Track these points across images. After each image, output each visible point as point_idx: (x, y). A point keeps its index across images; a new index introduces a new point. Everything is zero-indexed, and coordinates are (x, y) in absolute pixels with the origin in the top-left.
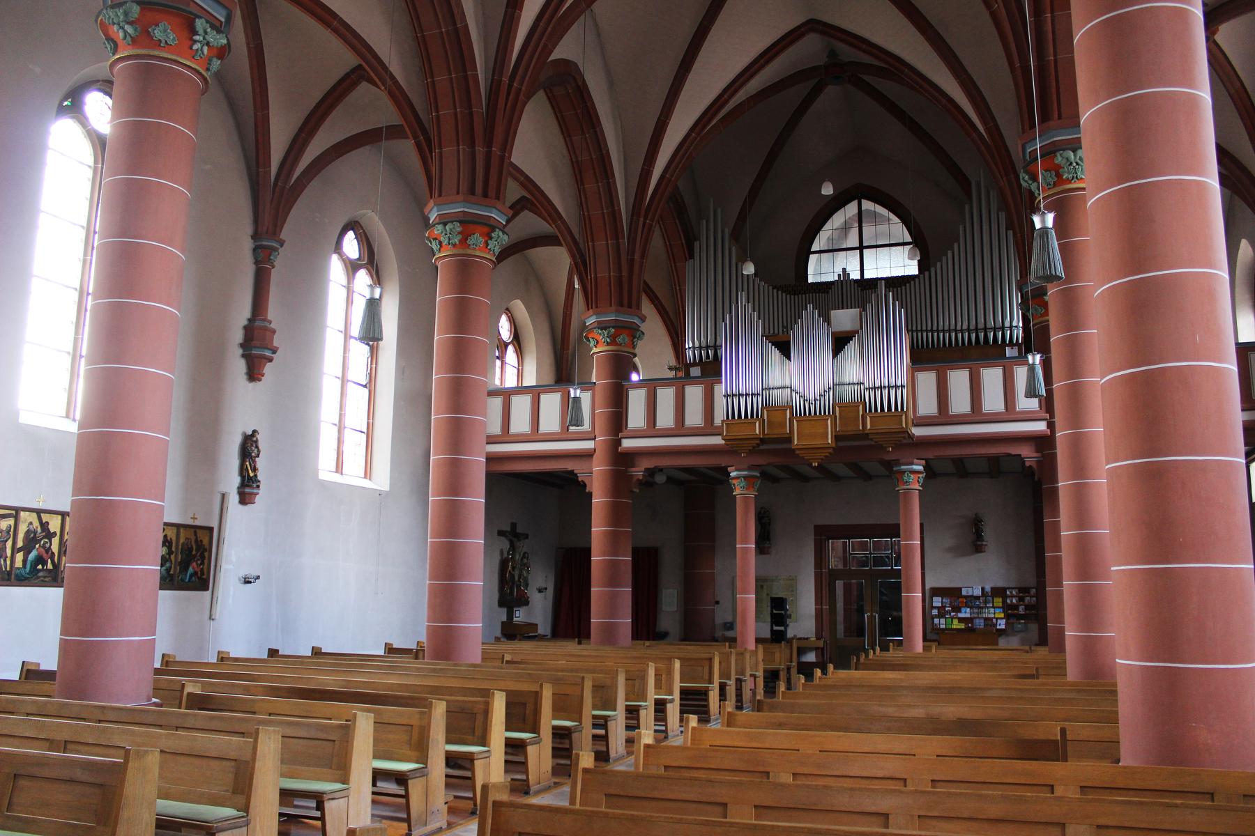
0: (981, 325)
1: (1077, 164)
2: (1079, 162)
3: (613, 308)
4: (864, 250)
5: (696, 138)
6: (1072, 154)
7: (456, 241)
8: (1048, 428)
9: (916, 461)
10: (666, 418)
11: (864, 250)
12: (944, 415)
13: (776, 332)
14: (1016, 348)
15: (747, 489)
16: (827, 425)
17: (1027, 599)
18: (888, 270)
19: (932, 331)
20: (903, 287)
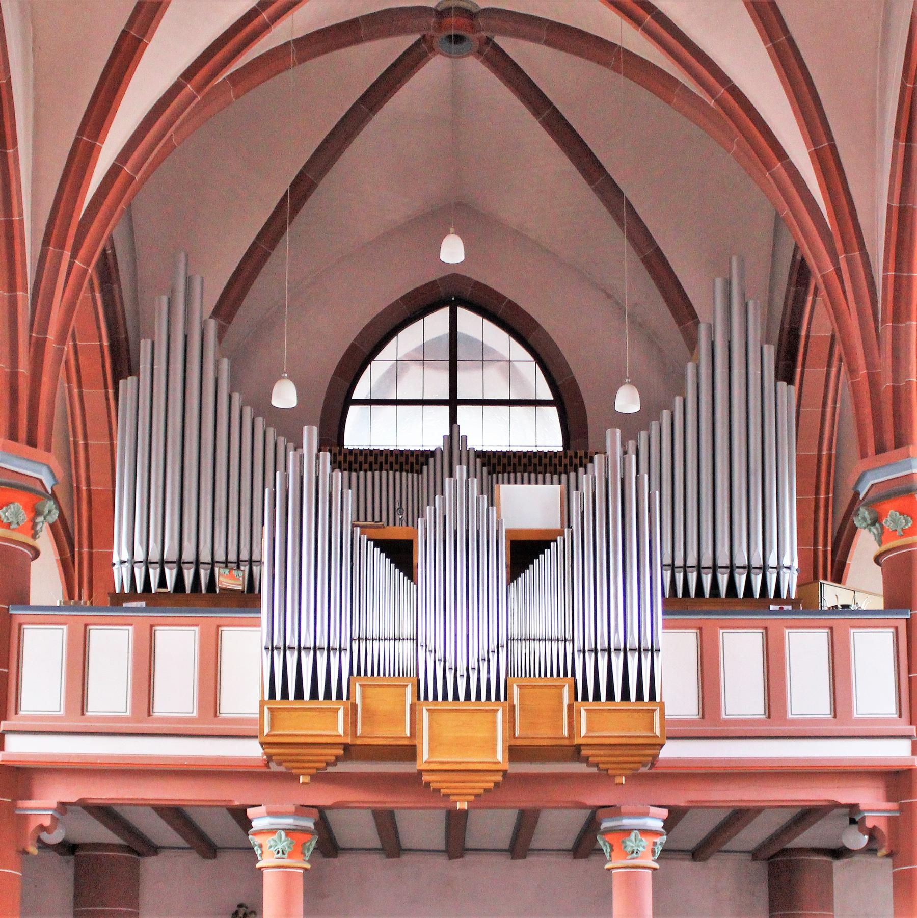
0: (723, 560)
16: (495, 722)
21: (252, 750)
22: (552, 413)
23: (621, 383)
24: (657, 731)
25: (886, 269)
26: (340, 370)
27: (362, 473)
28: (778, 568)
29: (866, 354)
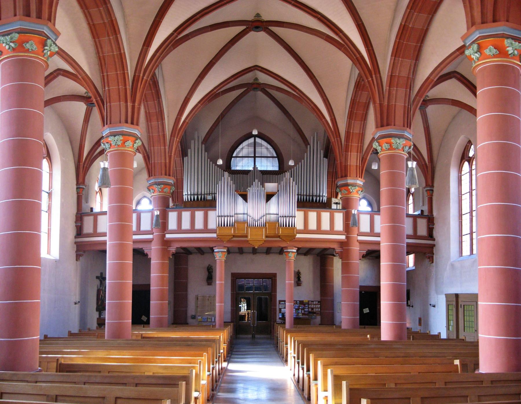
7: (119, 143)
18: (266, 167)
20: (280, 175)
21: (214, 235)
25: (344, 142)
29: (340, 158)
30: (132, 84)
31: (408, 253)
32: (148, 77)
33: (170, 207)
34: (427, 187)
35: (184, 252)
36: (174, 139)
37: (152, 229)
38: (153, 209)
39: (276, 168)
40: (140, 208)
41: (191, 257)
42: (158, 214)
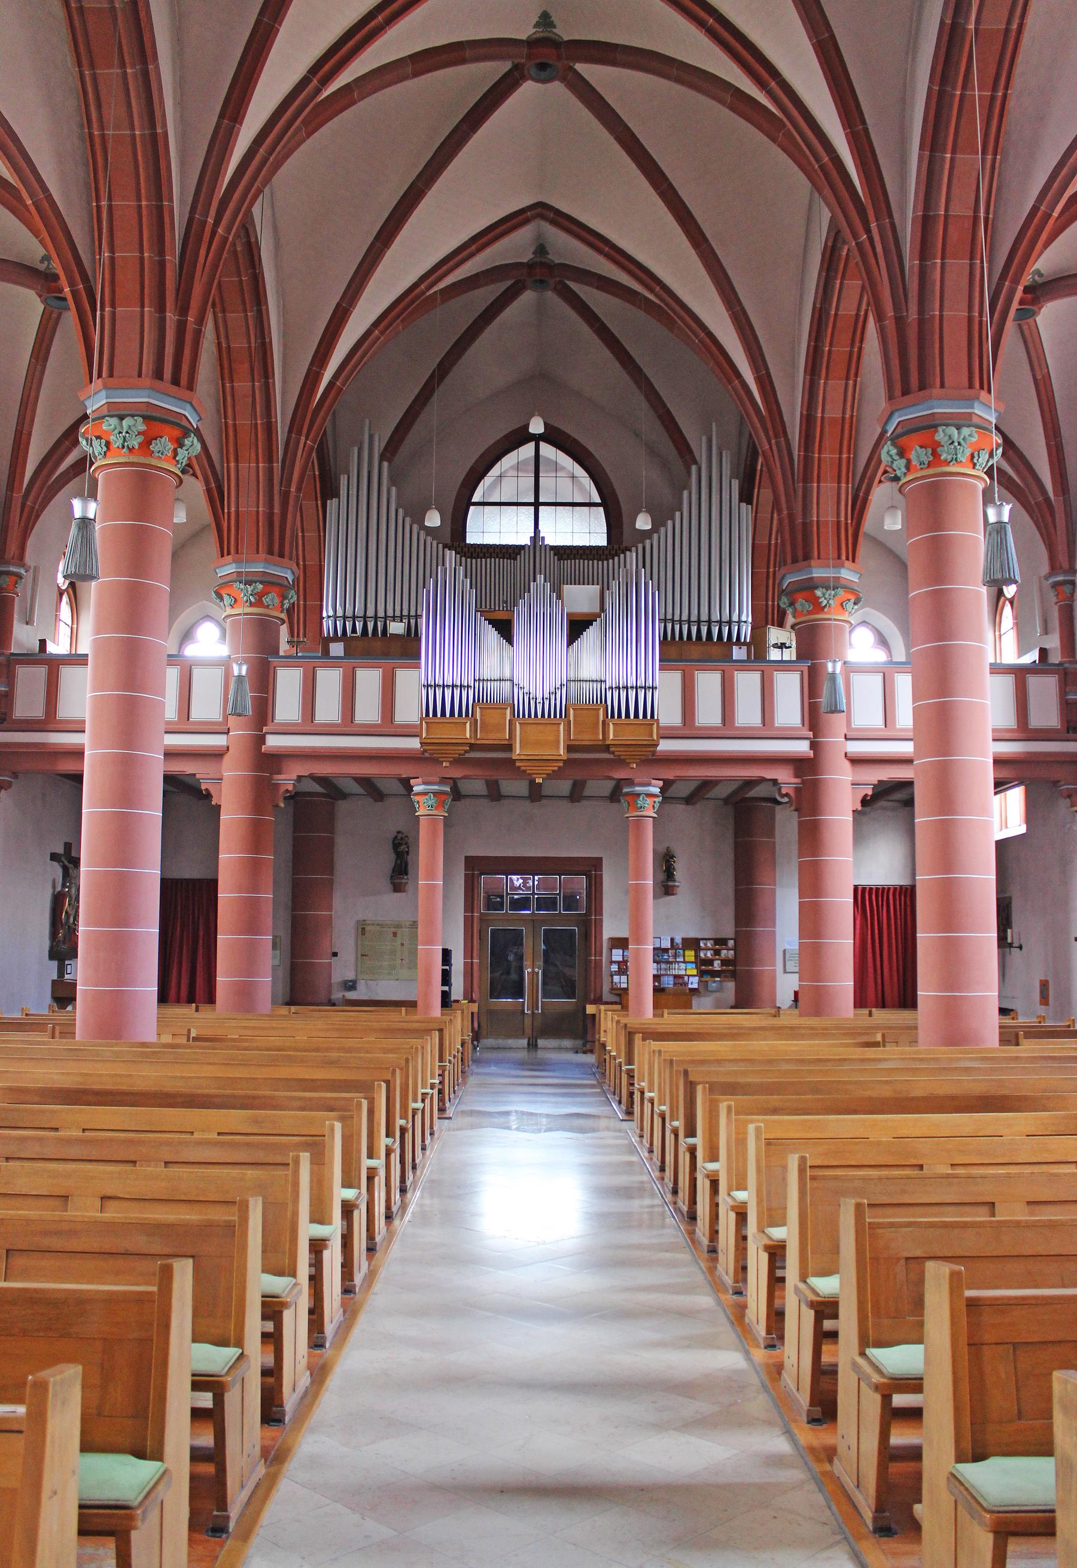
0: (704, 617)
1: (959, 444)
2: (962, 442)
3: (263, 555)
4: (540, 508)
5: (378, 338)
6: (956, 432)
7: (135, 442)
8: (811, 749)
9: (654, 782)
10: (328, 710)
11: (540, 508)
12: (688, 728)
13: (493, 607)
14: (744, 648)
15: (436, 809)
16: (559, 731)
17: (724, 953)
19: (680, 621)
20: (611, 561)
22: (601, 509)
23: (640, 511)
24: (655, 737)
26: (464, 484)
27: (479, 560)
28: (739, 622)
30: (183, 244)
31: (1000, 785)
32: (229, 230)
33: (281, 653)
34: (1057, 574)
35: (325, 791)
36: (298, 442)
37: (226, 717)
38: (229, 657)
39: (601, 540)
40: (191, 651)
41: (342, 806)
42: (244, 673)
